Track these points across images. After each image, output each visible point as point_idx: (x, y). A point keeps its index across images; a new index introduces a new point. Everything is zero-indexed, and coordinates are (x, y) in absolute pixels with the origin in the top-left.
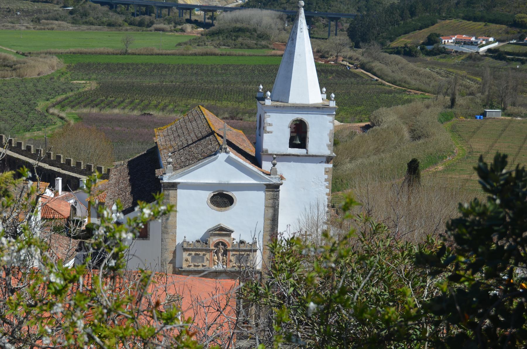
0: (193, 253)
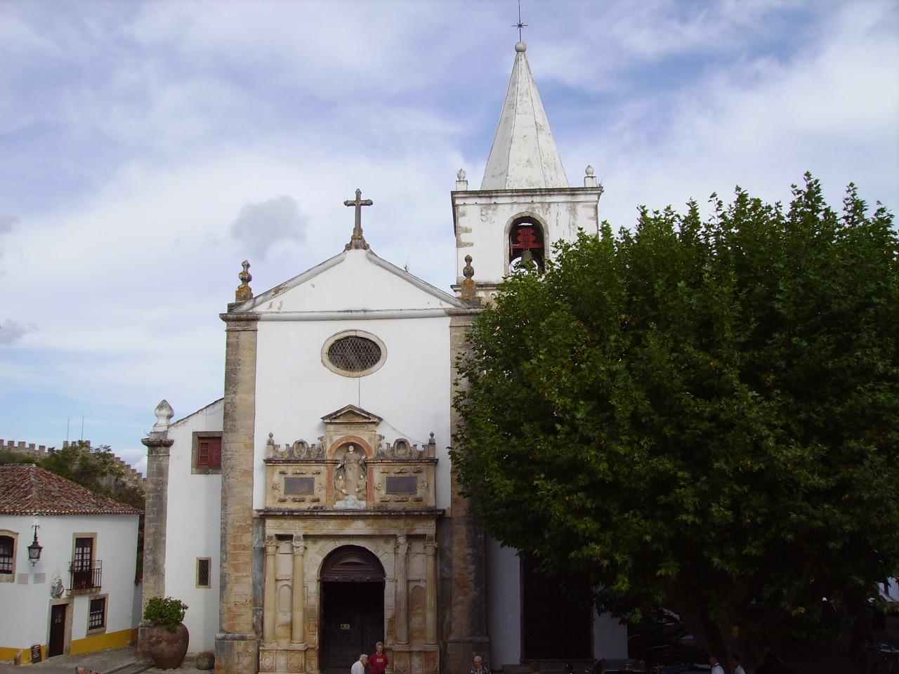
0: (290, 470)
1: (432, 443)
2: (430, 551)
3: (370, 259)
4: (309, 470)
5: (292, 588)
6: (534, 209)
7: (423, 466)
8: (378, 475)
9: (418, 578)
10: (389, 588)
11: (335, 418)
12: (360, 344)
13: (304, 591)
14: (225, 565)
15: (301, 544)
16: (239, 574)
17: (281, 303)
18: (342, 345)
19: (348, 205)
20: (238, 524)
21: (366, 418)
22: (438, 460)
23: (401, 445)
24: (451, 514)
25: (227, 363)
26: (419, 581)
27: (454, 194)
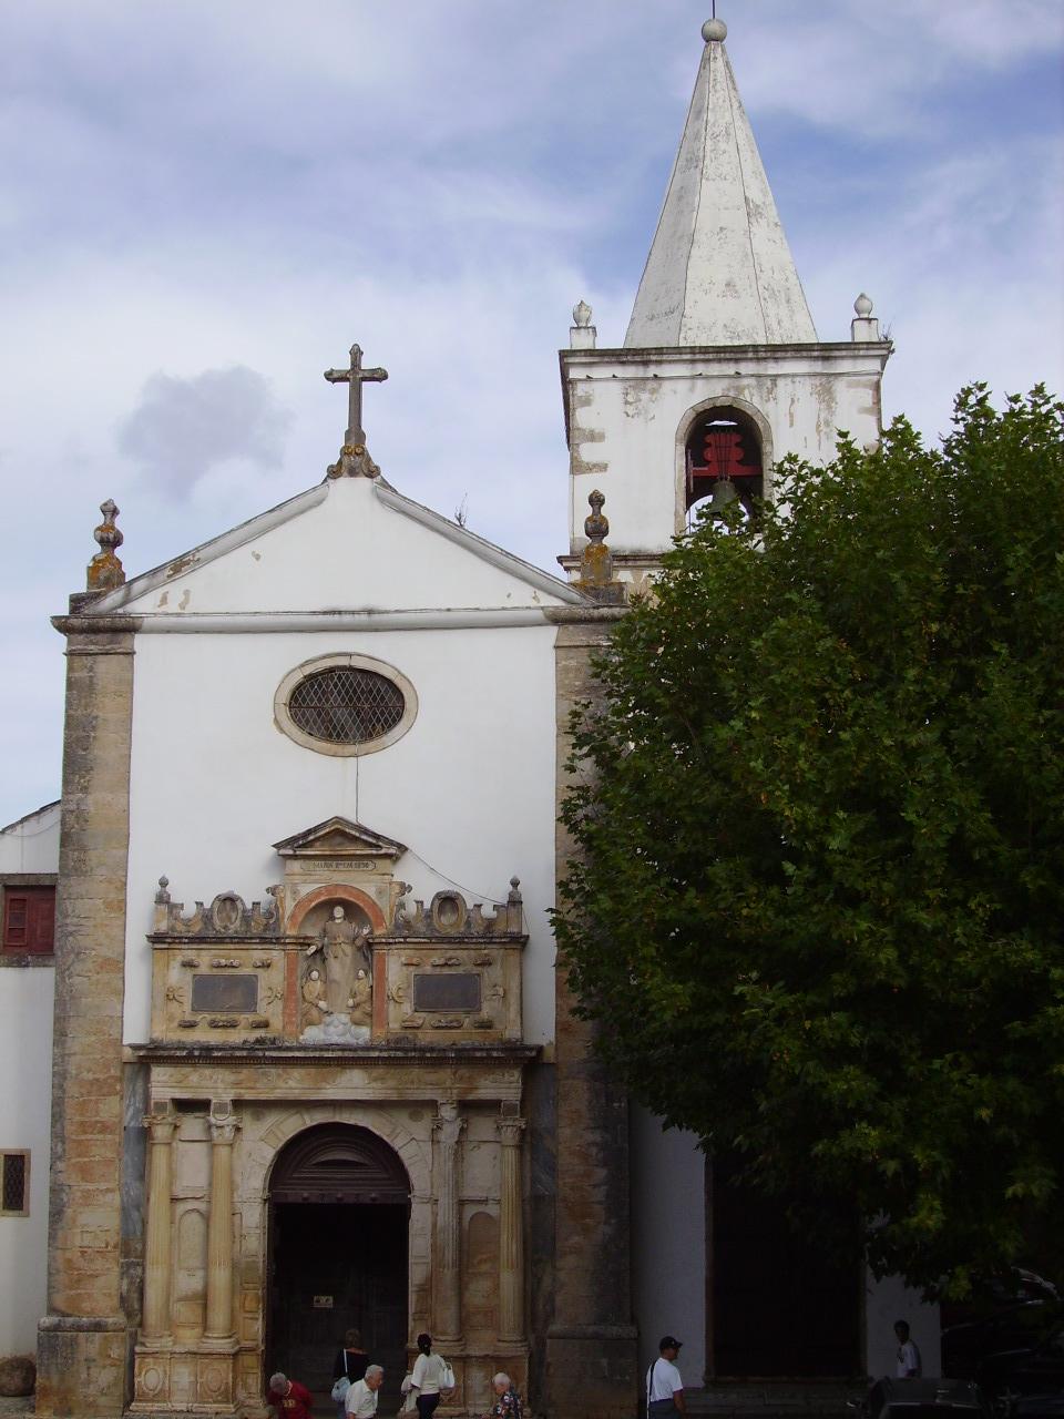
0: (205, 958)
1: (515, 902)
2: (510, 1136)
3: (382, 500)
4: (246, 960)
5: (207, 1218)
6: (740, 390)
7: (495, 952)
8: (397, 970)
9: (481, 1195)
10: (420, 1219)
11: (300, 847)
12: (359, 684)
13: (233, 1225)
14: (60, 1165)
15: (229, 1119)
16: (91, 1187)
17: (187, 593)
18: (320, 686)
19: (334, 381)
20: (90, 1076)
21: (371, 845)
22: (528, 936)
23: (448, 907)
24: (556, 1058)
25: (68, 726)
26: (485, 1201)
27: (563, 354)
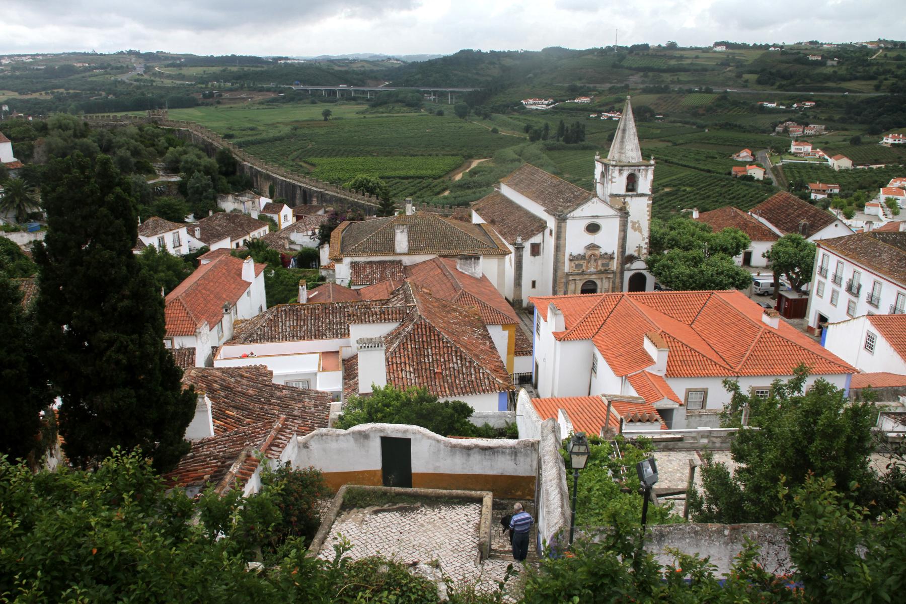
4: (581, 262)
8: (600, 263)
